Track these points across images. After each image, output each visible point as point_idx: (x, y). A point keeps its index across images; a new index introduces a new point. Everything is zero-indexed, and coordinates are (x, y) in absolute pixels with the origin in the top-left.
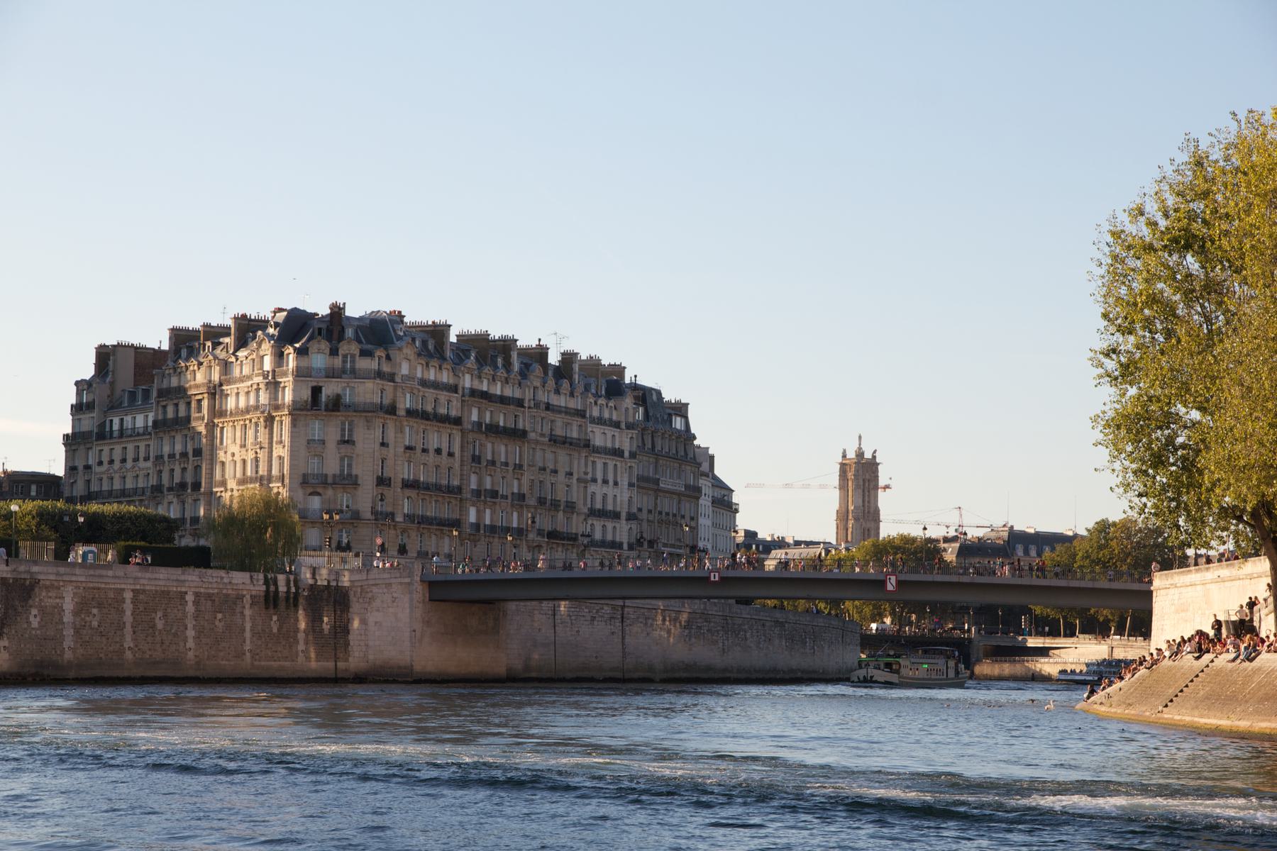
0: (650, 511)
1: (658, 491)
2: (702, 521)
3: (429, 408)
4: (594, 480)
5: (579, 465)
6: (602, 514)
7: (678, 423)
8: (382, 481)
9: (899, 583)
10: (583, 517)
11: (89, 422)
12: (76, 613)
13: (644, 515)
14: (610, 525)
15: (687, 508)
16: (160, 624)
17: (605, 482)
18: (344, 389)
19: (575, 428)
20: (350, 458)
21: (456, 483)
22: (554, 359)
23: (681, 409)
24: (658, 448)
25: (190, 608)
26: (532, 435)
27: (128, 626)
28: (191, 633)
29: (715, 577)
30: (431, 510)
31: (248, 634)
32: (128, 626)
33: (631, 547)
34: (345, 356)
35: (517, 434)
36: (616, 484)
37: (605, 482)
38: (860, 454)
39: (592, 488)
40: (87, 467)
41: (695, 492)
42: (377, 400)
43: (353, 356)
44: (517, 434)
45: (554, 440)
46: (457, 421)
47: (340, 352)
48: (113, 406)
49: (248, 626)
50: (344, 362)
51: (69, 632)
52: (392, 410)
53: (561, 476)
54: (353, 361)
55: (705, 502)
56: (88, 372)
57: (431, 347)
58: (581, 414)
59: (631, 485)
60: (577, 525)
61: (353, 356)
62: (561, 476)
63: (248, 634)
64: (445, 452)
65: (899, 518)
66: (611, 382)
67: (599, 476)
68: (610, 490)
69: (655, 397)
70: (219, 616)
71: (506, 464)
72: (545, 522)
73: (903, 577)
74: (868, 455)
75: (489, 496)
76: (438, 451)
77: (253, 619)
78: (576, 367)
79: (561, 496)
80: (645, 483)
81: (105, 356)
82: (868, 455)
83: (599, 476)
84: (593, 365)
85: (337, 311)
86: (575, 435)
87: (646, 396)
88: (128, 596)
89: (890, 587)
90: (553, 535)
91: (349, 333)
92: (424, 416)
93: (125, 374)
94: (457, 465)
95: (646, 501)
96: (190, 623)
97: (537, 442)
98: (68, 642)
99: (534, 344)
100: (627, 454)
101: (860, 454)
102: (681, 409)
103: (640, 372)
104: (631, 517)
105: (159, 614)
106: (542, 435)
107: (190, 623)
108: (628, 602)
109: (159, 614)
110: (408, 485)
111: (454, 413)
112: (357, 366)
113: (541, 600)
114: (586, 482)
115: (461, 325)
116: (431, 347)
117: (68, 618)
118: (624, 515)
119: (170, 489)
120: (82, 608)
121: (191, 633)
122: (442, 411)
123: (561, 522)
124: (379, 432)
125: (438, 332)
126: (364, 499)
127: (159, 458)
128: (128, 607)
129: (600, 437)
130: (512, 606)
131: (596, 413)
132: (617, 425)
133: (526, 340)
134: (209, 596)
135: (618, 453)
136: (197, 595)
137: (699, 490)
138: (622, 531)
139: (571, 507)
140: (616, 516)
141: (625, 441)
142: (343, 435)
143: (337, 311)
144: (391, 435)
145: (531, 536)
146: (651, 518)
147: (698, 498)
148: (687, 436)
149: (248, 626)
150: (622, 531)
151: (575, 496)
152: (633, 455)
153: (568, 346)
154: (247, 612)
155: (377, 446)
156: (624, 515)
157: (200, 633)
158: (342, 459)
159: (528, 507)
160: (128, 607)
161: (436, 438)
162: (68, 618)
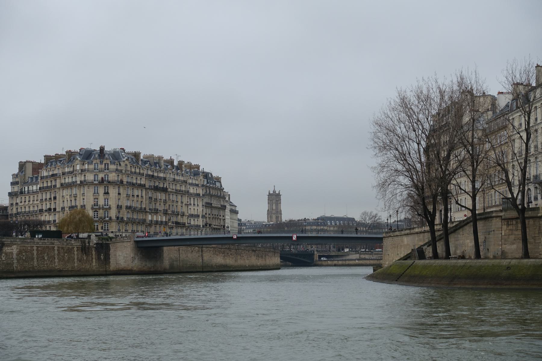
0: (209, 214)
2: (226, 217)
3: (135, 181)
4: (191, 204)
5: (185, 199)
7: (218, 184)
8: (119, 207)
9: (297, 237)
11: (16, 189)
12: (18, 255)
13: (207, 216)
14: (196, 220)
15: (221, 213)
16: (46, 258)
17: (194, 205)
18: (105, 175)
19: (184, 187)
20: (108, 199)
21: (144, 206)
22: (176, 163)
24: (211, 193)
25: (56, 252)
26: (169, 190)
27: (35, 258)
28: (56, 260)
29: (235, 237)
30: (135, 216)
31: (76, 260)
32: (35, 258)
33: (203, 226)
34: (105, 164)
35: (164, 190)
36: (198, 205)
37: (194, 205)
38: (274, 192)
39: (189, 207)
40: (17, 204)
41: (224, 208)
42: (116, 179)
43: (108, 164)
44: (164, 190)
45: (177, 192)
46: (144, 186)
47: (104, 163)
48: (25, 183)
49: (76, 257)
50: (105, 166)
51: (15, 261)
52: (122, 182)
53: (179, 203)
54: (108, 166)
55: (227, 211)
56: (16, 171)
57: (134, 160)
58: (185, 182)
59: (203, 205)
60: (185, 220)
61: (108, 164)
62: (179, 203)
63: (76, 260)
64: (140, 196)
65: (288, 214)
66: (194, 171)
67: (192, 203)
68: (196, 208)
70: (66, 254)
71: (161, 200)
72: (174, 219)
73: (298, 235)
74: (277, 192)
75: (156, 212)
76: (138, 196)
77: (77, 255)
78: (183, 166)
79: (180, 209)
80: (208, 205)
81: (22, 166)
82: (277, 192)
83: (192, 203)
84: (189, 166)
85: (102, 149)
86: (184, 189)
87: (206, 175)
88: (35, 248)
89: (294, 239)
90: (177, 223)
91: (107, 156)
92: (133, 184)
93: (29, 172)
94: (144, 200)
95: (209, 211)
96: (56, 257)
97: (171, 192)
98: (15, 265)
99: (169, 158)
100: (201, 195)
101: (274, 192)
103: (205, 167)
104: (203, 217)
105: (46, 255)
106: (173, 189)
107: (56, 257)
108: (204, 246)
109: (46, 255)
110: (128, 208)
111: (142, 183)
112: (109, 167)
113: (175, 246)
114: (188, 205)
115: (144, 152)
116: (134, 160)
117: (15, 256)
119: (46, 211)
120: (20, 253)
121: (56, 260)
122: (139, 182)
123: (180, 219)
124: (117, 190)
125: (136, 155)
126: (113, 213)
127: (42, 200)
128: (35, 253)
129: (192, 190)
130: (165, 249)
131: (190, 181)
132: (197, 185)
133: (166, 157)
134: (62, 248)
135: (198, 195)
136: (58, 247)
137: (225, 206)
138: (200, 222)
139: (183, 215)
141: (200, 191)
142: (105, 191)
143: (102, 149)
144: (121, 191)
145: (170, 224)
148: (221, 189)
149: (76, 257)
150: (200, 222)
151: (184, 209)
152: (203, 195)
153: (180, 159)
154: (76, 253)
155: (117, 195)
157: (59, 260)
158: (105, 199)
159: (168, 214)
160: (35, 253)
161: (136, 192)
162: (15, 256)
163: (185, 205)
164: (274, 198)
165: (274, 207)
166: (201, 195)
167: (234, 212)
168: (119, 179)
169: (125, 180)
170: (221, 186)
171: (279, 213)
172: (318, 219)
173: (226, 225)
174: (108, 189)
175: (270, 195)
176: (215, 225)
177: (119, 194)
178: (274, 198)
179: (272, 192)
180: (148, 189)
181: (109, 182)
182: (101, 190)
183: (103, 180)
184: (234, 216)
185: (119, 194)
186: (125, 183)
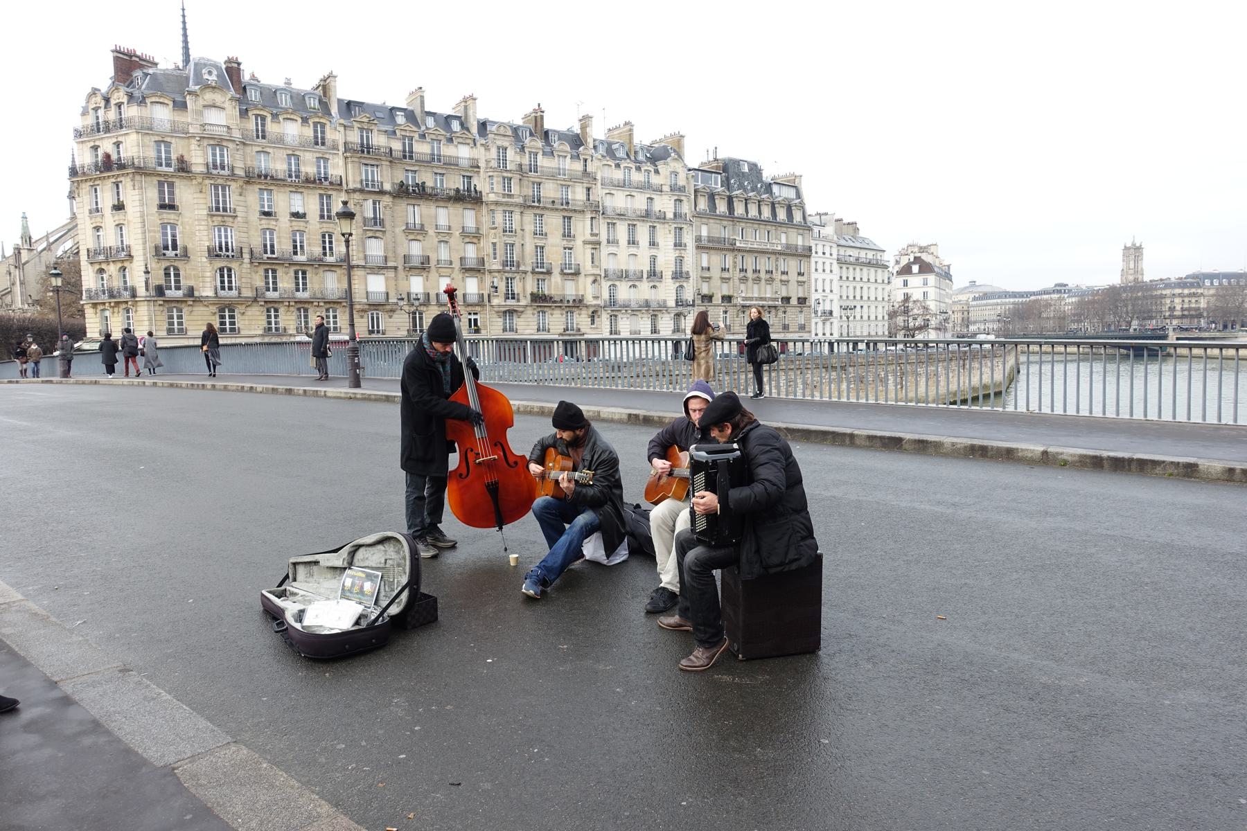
1: (734, 249)
15: (792, 265)
23: (792, 183)
36: (653, 244)
37: (632, 242)
38: (1134, 245)
52: (183, 168)
65: (1151, 271)
97: (497, 203)
101: (1134, 245)
102: (792, 183)
118: (668, 275)
123: (555, 286)
145: (495, 301)
146: (726, 275)
147: (809, 257)
151: (582, 256)
159: (490, 272)
163: (585, 243)
164: (1134, 252)
165: (1132, 266)
166: (670, 215)
168: (174, 156)
169: (198, 158)
170: (799, 195)
172: (1187, 277)
173: (814, 297)
174: (171, 193)
175: (1126, 248)
176: (745, 299)
177: (167, 206)
178: (1134, 252)
179: (1129, 245)
180: (355, 191)
181: (122, 166)
182: (107, 198)
183: (108, 165)
185: (167, 206)
186: (198, 168)
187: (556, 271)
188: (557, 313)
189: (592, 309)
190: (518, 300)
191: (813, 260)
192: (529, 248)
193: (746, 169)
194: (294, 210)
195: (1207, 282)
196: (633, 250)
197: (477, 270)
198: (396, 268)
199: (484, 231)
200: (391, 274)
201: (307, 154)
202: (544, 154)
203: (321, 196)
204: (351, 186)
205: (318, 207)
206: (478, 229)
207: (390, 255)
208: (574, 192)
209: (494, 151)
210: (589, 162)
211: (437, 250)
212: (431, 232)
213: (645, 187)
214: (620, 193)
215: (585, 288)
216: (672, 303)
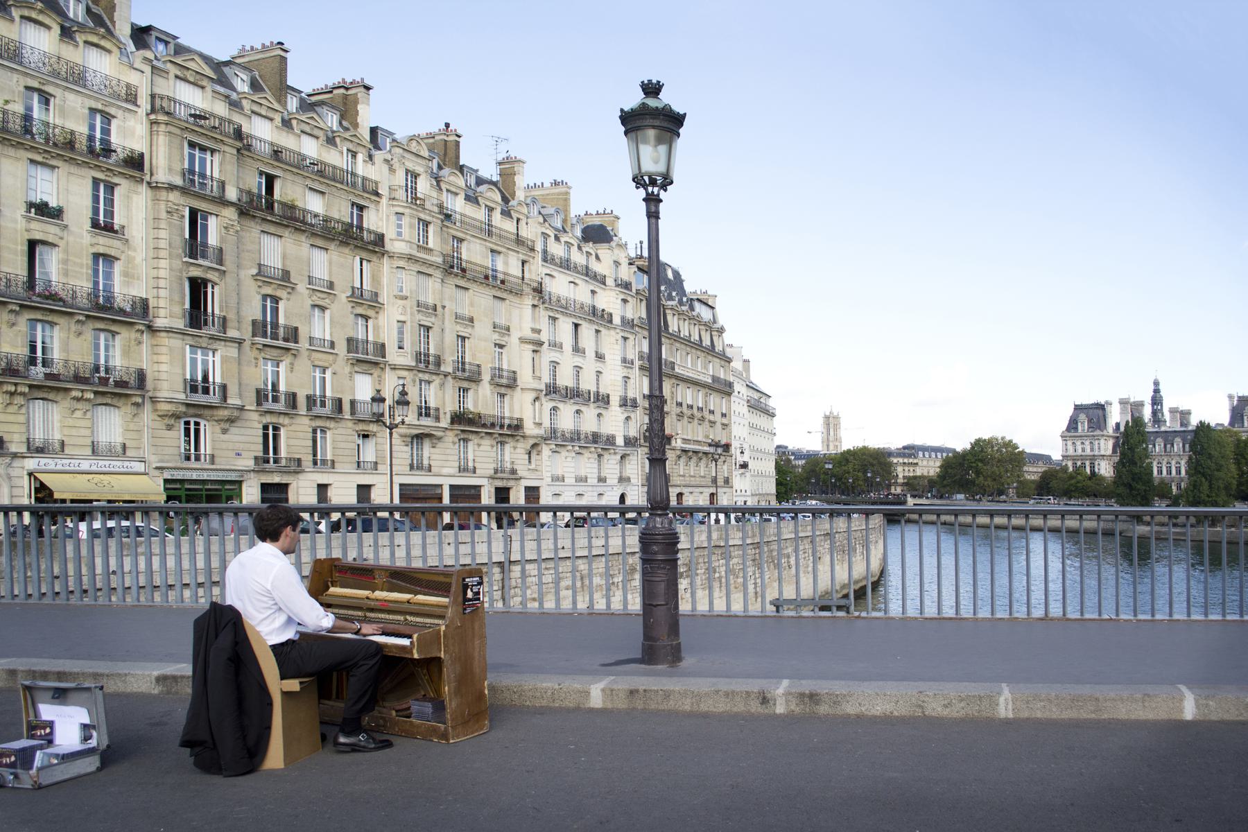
5: (523, 317)
6: (574, 394)
10: (533, 395)
15: (715, 401)
17: (577, 349)
37: (577, 349)
41: (724, 389)
69: (670, 275)
76: (42, 209)
118: (615, 400)
123: (482, 400)
137: (730, 385)
139: (506, 384)
140: (602, 400)
147: (729, 394)
148: (715, 329)
151: (518, 359)
156: (615, 400)
159: (394, 368)
163: (523, 340)
167: (760, 406)
171: (838, 439)
176: (685, 441)
184: (761, 421)
187: (486, 377)
188: (487, 443)
189: (532, 442)
190: (438, 419)
191: (733, 398)
192: (450, 338)
193: (670, 275)
194: (37, 198)
195: (921, 454)
196: (578, 361)
197: (369, 358)
198: (240, 342)
199: (384, 298)
200: (232, 351)
201: (71, 97)
202: (468, 198)
203: (96, 182)
204: (162, 176)
205: (88, 202)
206: (376, 294)
207: (231, 316)
208: (506, 263)
209: (401, 174)
210: (523, 223)
211: (309, 319)
212: (302, 287)
213: (587, 273)
214: (562, 276)
215: (521, 406)
216: (620, 441)
